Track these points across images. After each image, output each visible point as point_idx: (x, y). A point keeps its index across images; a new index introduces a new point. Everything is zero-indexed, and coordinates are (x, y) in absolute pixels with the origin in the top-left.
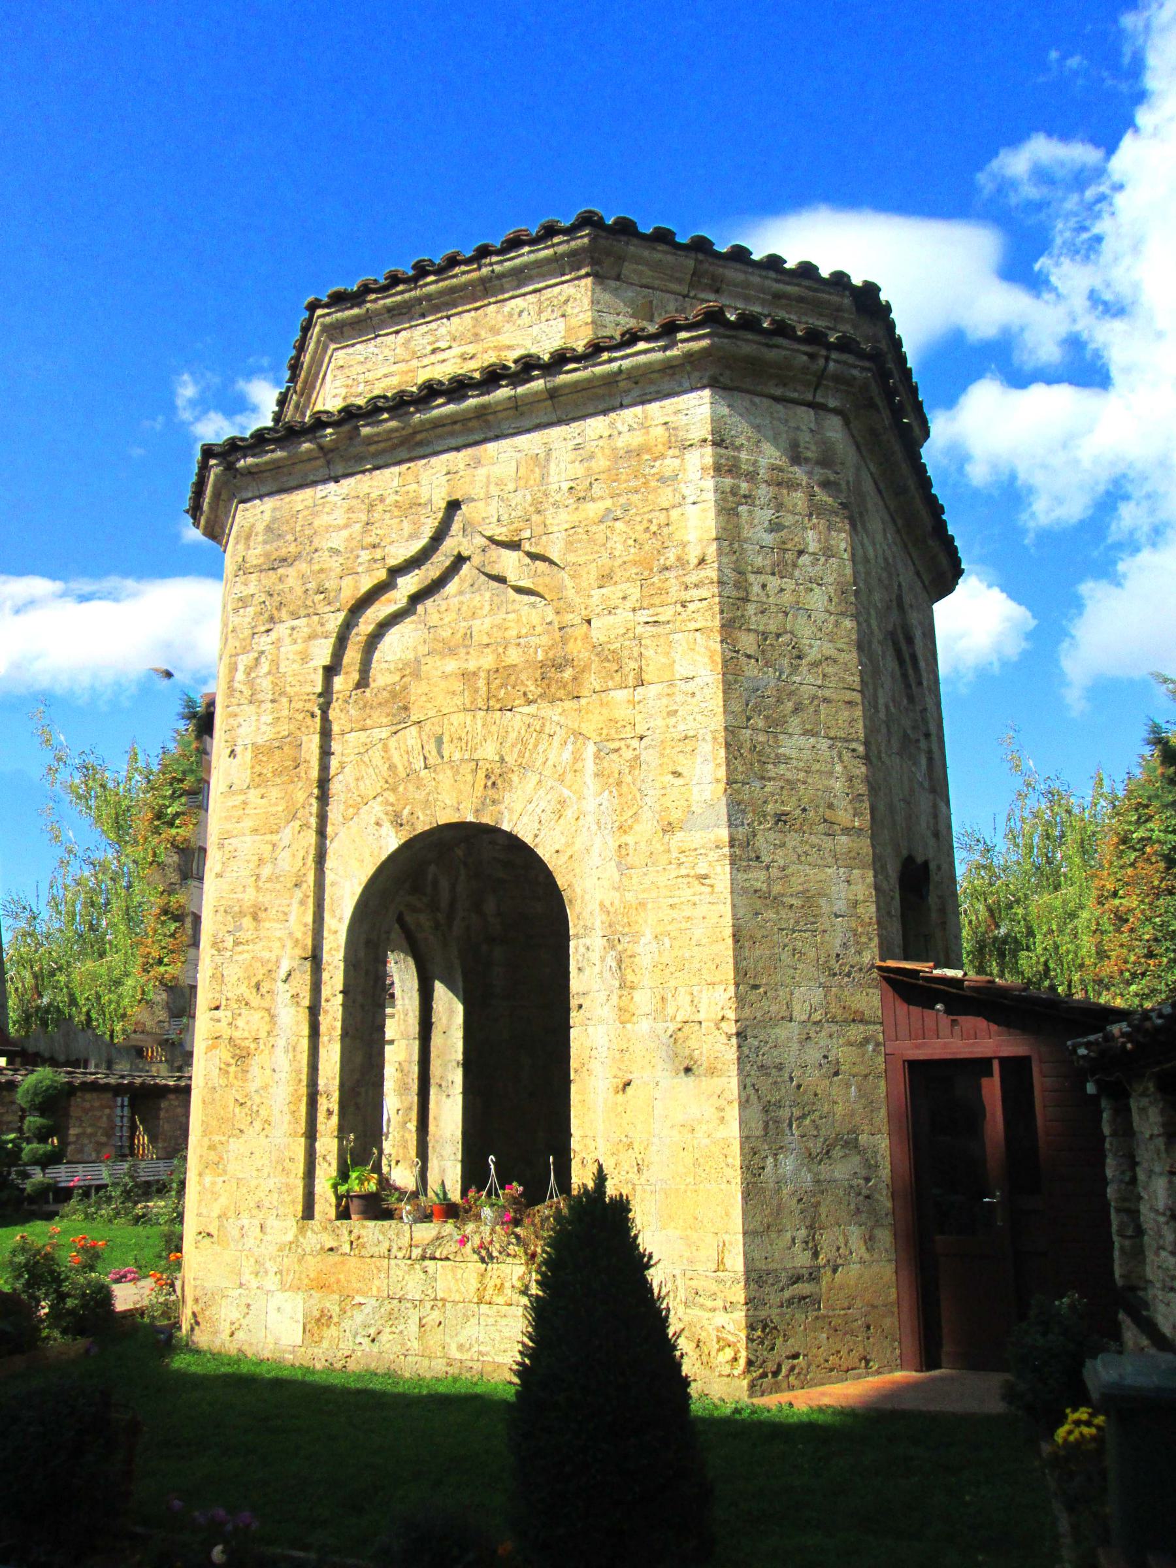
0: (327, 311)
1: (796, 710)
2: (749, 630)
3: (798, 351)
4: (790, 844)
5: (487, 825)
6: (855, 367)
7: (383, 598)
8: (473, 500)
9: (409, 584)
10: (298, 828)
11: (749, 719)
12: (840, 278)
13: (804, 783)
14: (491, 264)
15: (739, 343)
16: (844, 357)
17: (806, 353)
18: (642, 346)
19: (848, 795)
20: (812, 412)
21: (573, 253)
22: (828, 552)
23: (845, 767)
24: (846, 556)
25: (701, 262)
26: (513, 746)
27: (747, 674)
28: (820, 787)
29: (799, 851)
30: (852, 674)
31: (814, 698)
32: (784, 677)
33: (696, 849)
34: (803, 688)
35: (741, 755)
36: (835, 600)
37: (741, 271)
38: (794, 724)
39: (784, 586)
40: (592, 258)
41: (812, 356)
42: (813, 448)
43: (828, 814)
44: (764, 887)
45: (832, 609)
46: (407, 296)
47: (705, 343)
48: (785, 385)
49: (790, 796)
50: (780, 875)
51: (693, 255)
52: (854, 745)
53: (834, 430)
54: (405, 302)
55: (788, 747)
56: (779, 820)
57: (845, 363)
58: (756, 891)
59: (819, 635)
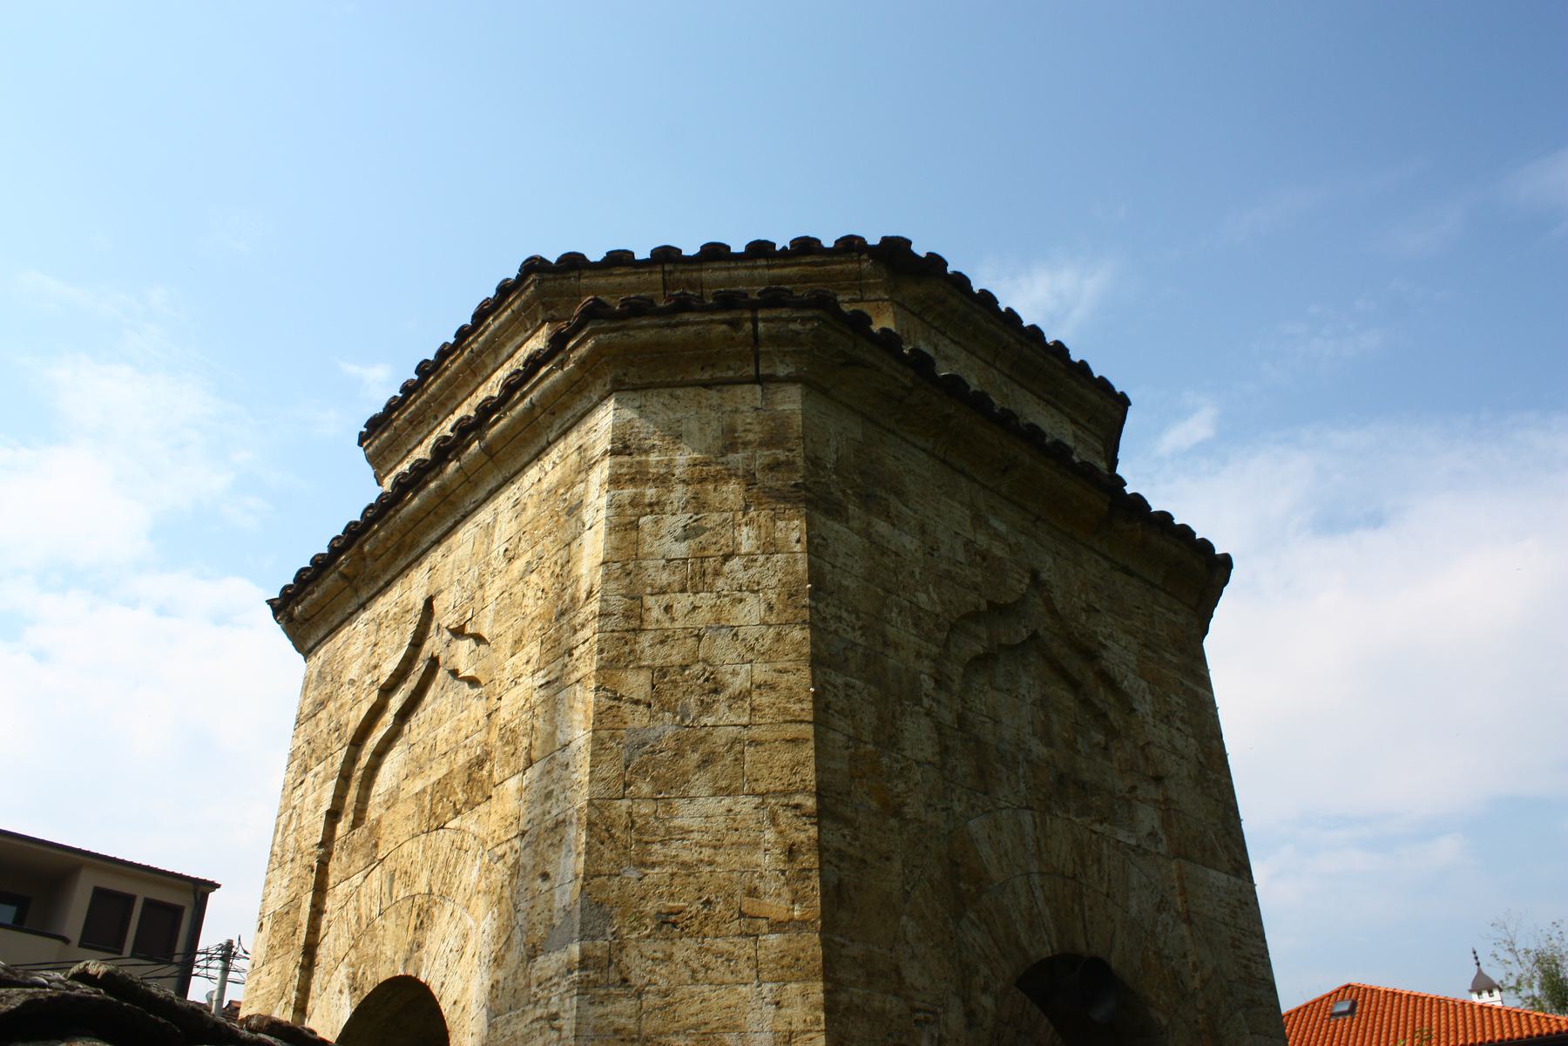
0: (368, 441)
1: (704, 763)
2: (640, 668)
3: (711, 321)
4: (679, 955)
5: (410, 976)
6: (794, 320)
7: (380, 723)
8: (441, 592)
9: (396, 702)
10: (283, 1007)
11: (627, 785)
12: (851, 245)
13: (710, 863)
14: (469, 345)
15: (631, 333)
16: (775, 313)
17: (723, 322)
18: (544, 370)
19: (783, 873)
20: (758, 388)
21: (526, 306)
22: (770, 547)
23: (781, 833)
24: (798, 548)
25: (670, 272)
26: (440, 871)
27: (630, 725)
28: (737, 866)
29: (695, 965)
30: (800, 701)
31: (735, 741)
32: (687, 722)
33: (551, 978)
34: (720, 732)
35: (611, 836)
36: (778, 607)
37: (721, 269)
38: (700, 783)
39: (697, 603)
40: (543, 304)
41: (734, 324)
42: (757, 428)
43: (748, 905)
44: (631, 1025)
45: (773, 619)
46: (418, 403)
47: (590, 343)
48: (713, 366)
49: (684, 886)
50: (659, 1002)
51: (659, 269)
52: (798, 799)
53: (790, 402)
54: (418, 409)
55: (687, 815)
56: (664, 923)
57: (779, 319)
58: (616, 1031)
59: (749, 656)
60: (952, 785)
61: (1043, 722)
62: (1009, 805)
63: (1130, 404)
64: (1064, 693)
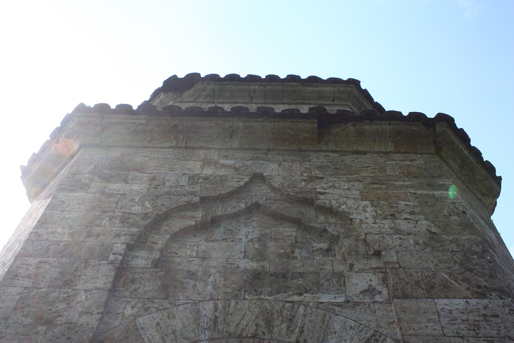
60: (129, 300)
61: (257, 249)
62: (189, 301)
63: (360, 82)
64: (286, 229)
